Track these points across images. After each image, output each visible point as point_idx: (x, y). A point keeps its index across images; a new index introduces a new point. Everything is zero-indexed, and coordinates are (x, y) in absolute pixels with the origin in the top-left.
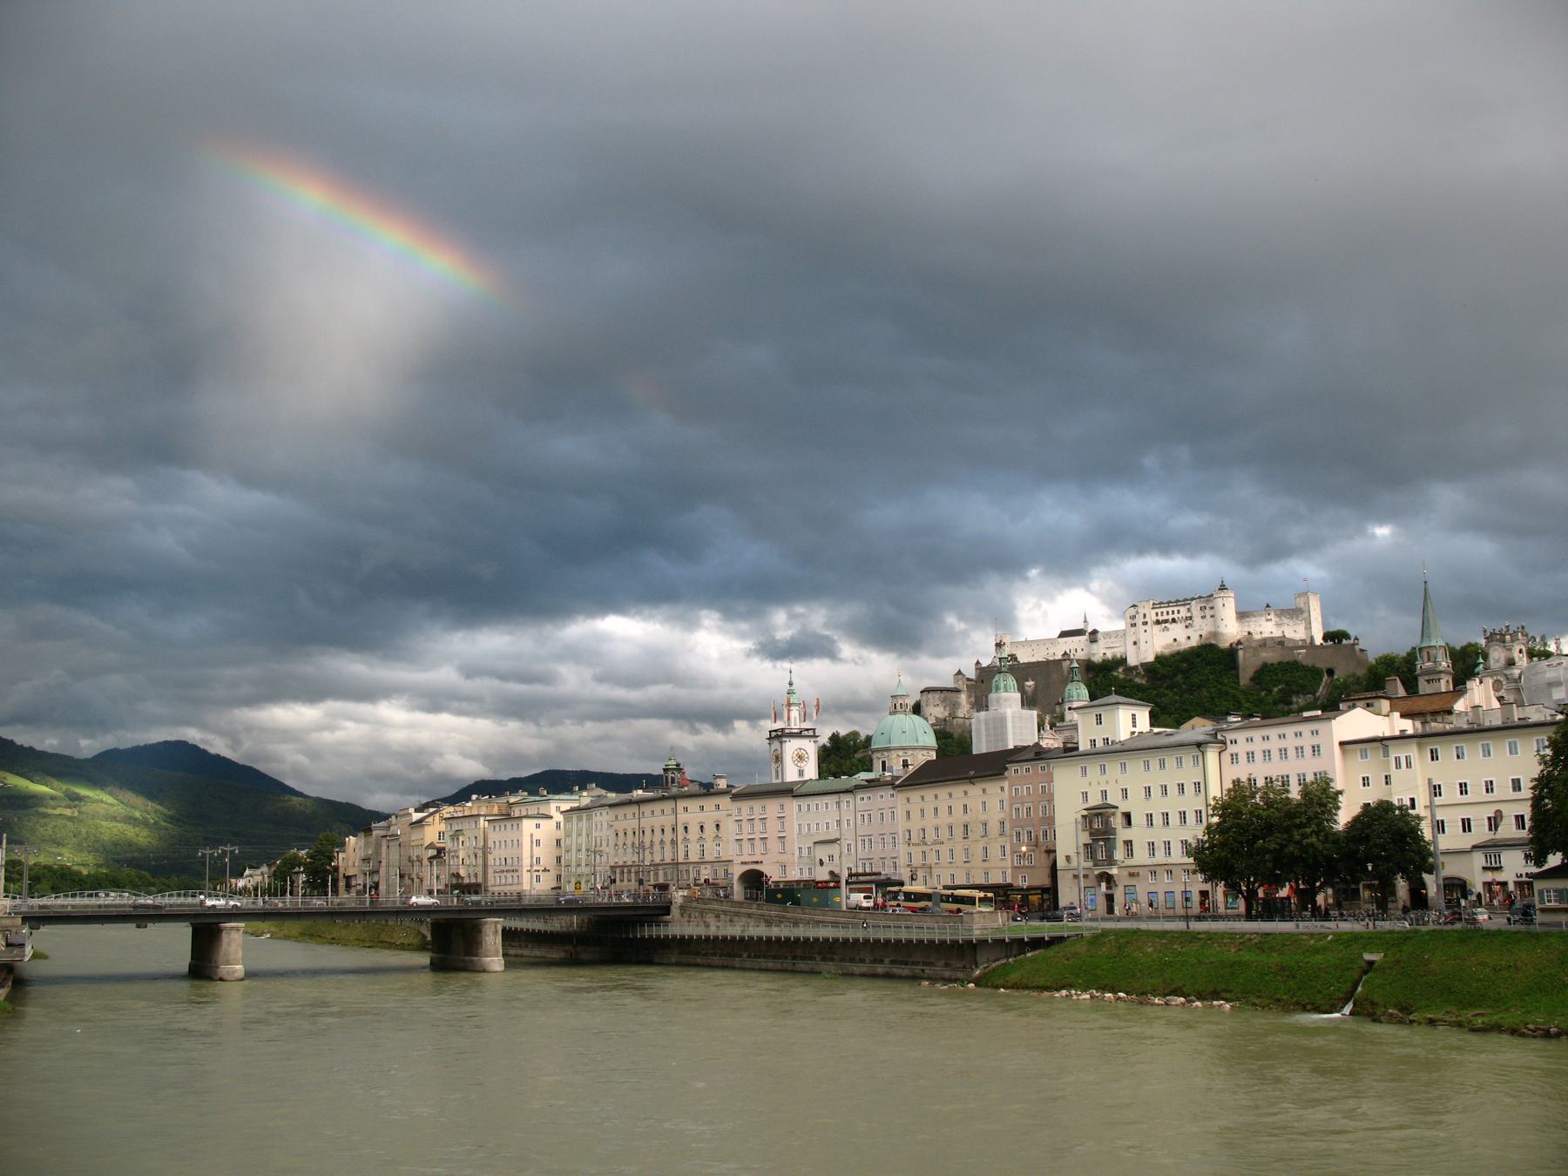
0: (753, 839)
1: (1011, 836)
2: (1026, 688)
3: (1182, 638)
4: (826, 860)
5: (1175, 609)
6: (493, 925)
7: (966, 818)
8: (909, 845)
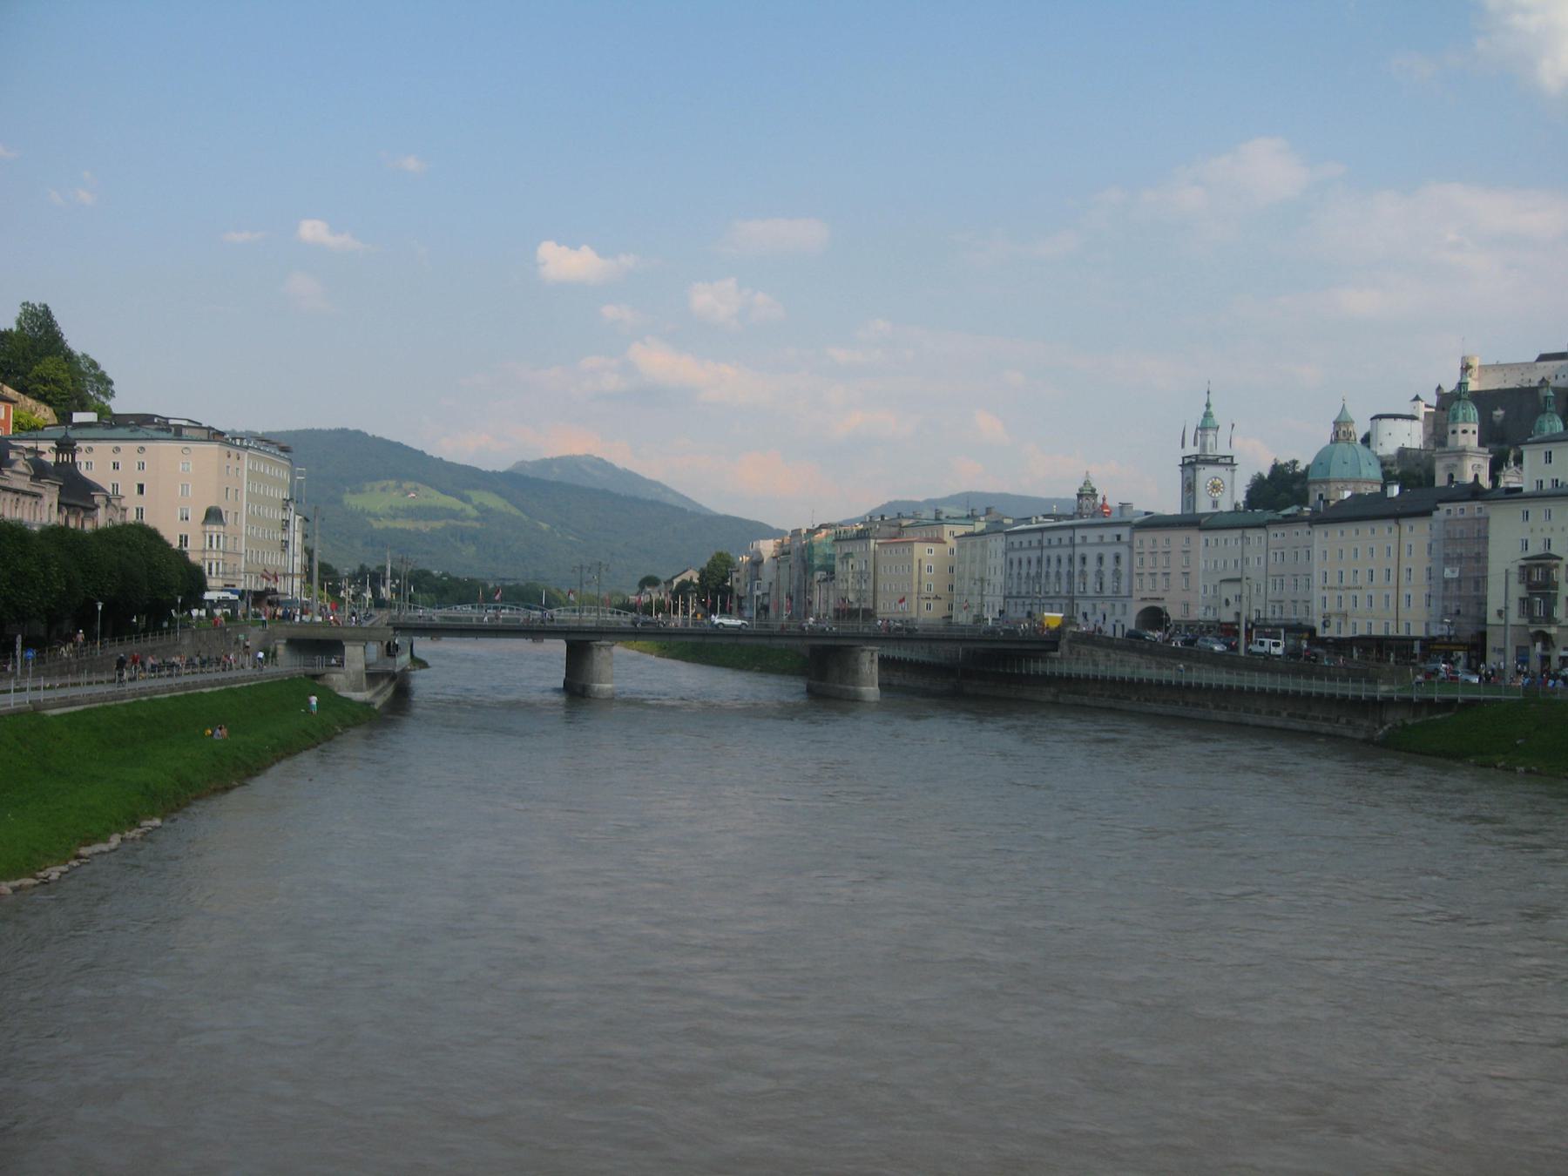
0: (1155, 574)
4: (1232, 600)
6: (870, 654)
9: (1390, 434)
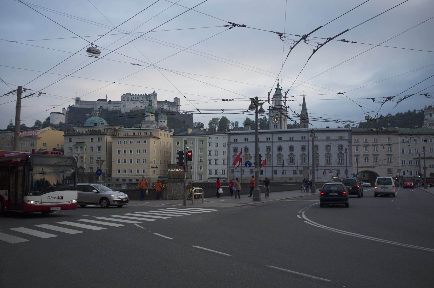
2: (87, 116)
3: (139, 106)
5: (138, 97)
9: (57, 118)
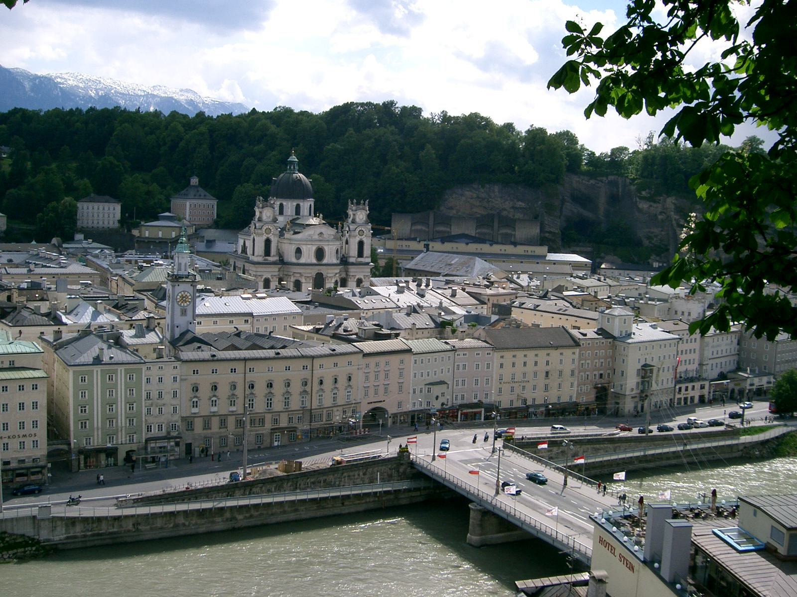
1: (578, 377)
7: (548, 368)
8: (500, 383)
